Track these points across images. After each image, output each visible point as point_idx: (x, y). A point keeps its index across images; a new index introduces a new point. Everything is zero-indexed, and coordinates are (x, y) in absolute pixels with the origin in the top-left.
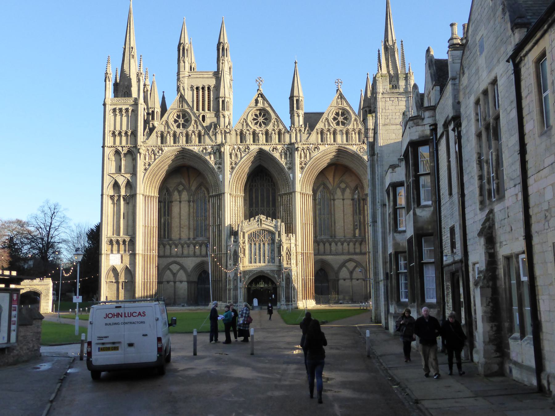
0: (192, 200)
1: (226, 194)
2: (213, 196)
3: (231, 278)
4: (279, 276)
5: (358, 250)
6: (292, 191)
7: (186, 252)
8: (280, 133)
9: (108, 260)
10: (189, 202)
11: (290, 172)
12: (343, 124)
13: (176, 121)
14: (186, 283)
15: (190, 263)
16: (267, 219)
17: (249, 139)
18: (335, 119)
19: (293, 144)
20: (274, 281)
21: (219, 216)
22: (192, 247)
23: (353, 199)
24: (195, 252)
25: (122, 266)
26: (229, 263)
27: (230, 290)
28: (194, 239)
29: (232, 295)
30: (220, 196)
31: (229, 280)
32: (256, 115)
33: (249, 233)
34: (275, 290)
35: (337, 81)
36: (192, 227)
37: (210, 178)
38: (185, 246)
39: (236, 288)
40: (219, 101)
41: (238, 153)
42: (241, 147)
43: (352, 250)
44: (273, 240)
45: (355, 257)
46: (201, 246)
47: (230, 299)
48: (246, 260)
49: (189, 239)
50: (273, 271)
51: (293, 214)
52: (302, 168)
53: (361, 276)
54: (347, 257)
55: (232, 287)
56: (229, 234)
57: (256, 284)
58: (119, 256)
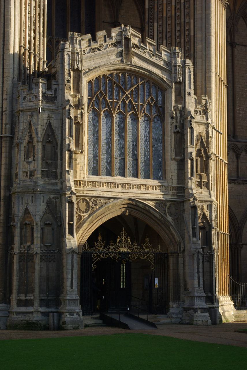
3: (37, 219)
4: (179, 219)
16: (143, 41)
20: (162, 234)
26: (22, 166)
27: (27, 258)
29: (37, 275)
31: (24, 226)
33: (92, 76)
34: (162, 260)
47: (26, 287)
48: (83, 161)
51: (199, 47)
55: (37, 247)
56: (16, 79)
57: (107, 244)
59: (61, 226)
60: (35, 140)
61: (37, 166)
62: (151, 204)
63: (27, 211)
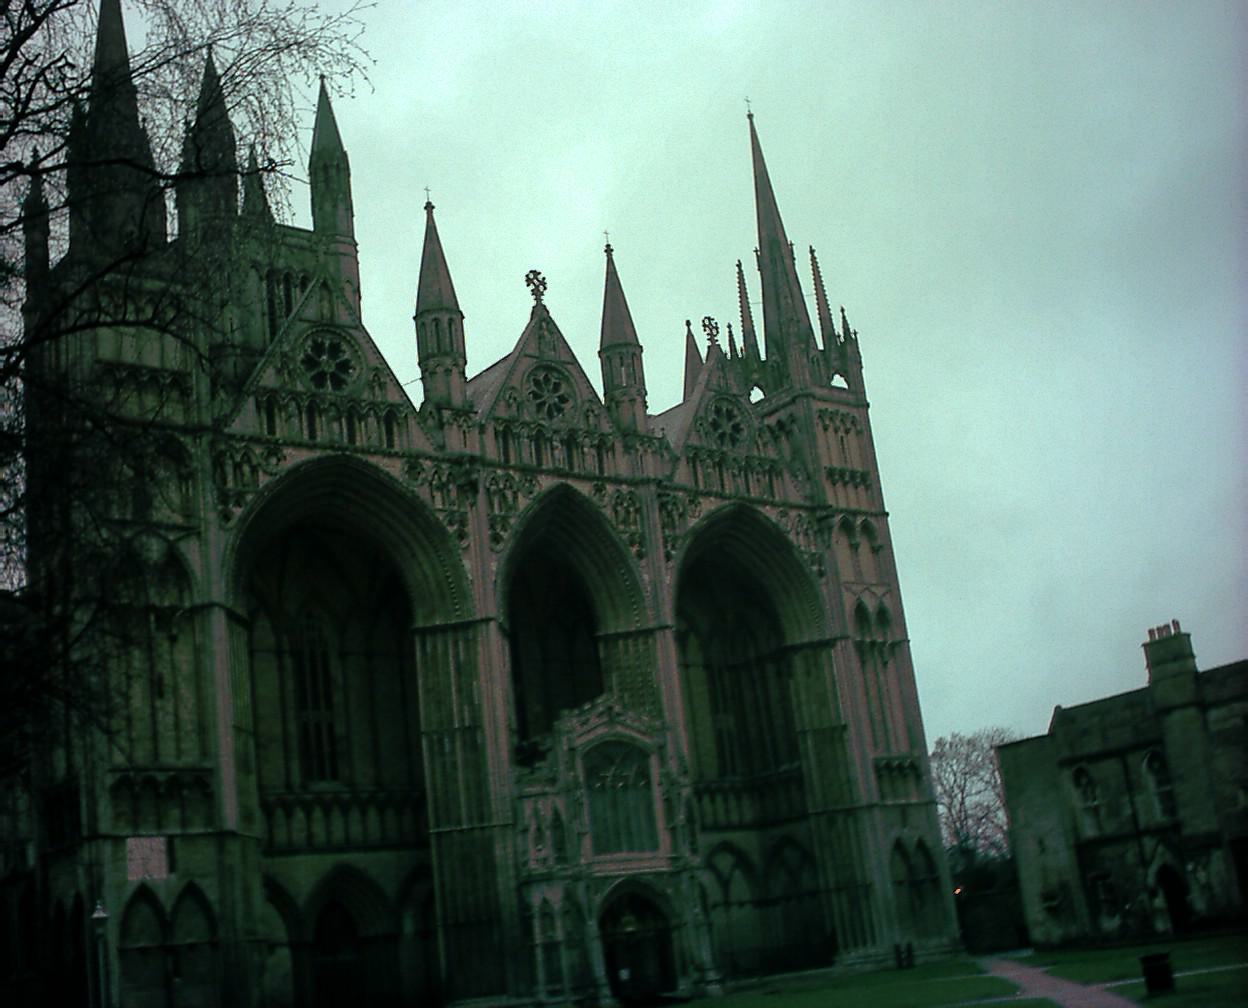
0: (286, 647)
1: (492, 625)
2: (434, 630)
5: (735, 818)
6: (652, 625)
7: (281, 836)
8: (602, 447)
9: (119, 859)
10: (279, 653)
11: (643, 562)
12: (734, 441)
13: (310, 362)
14: (284, 953)
15: (304, 874)
17: (526, 454)
18: (715, 425)
19: (646, 482)
21: (467, 695)
22: (300, 815)
23: (707, 667)
24: (310, 836)
25: (176, 882)
27: (551, 947)
28: (304, 787)
30: (466, 628)
32: (537, 383)
35: (707, 322)
36: (294, 743)
37: (420, 571)
38: (280, 813)
39: (576, 941)
40: (437, 321)
41: (509, 494)
42: (511, 472)
43: (722, 819)
44: (644, 774)
45: (737, 837)
46: (327, 813)
48: (587, 843)
49: (288, 786)
50: (659, 875)
51: (664, 699)
52: (668, 557)
53: (746, 896)
54: (716, 838)
55: (559, 935)
58: (160, 843)
59: (579, 911)
60: (543, 827)
61: (548, 851)
62: (650, 877)
63: (545, 901)
